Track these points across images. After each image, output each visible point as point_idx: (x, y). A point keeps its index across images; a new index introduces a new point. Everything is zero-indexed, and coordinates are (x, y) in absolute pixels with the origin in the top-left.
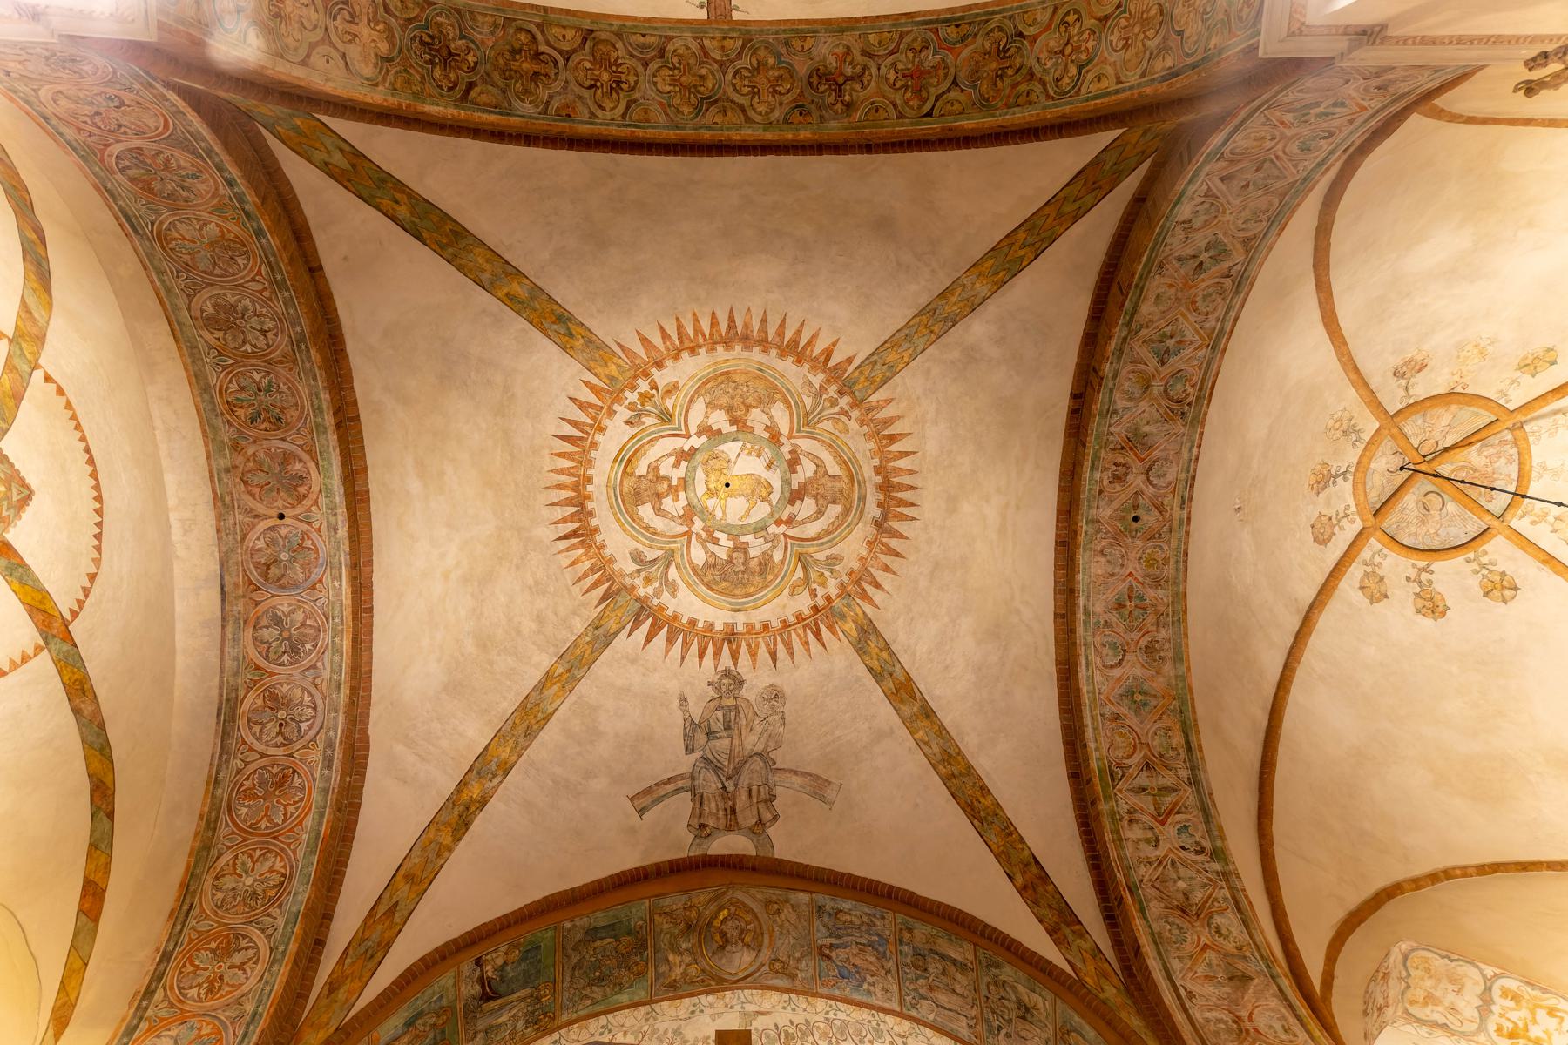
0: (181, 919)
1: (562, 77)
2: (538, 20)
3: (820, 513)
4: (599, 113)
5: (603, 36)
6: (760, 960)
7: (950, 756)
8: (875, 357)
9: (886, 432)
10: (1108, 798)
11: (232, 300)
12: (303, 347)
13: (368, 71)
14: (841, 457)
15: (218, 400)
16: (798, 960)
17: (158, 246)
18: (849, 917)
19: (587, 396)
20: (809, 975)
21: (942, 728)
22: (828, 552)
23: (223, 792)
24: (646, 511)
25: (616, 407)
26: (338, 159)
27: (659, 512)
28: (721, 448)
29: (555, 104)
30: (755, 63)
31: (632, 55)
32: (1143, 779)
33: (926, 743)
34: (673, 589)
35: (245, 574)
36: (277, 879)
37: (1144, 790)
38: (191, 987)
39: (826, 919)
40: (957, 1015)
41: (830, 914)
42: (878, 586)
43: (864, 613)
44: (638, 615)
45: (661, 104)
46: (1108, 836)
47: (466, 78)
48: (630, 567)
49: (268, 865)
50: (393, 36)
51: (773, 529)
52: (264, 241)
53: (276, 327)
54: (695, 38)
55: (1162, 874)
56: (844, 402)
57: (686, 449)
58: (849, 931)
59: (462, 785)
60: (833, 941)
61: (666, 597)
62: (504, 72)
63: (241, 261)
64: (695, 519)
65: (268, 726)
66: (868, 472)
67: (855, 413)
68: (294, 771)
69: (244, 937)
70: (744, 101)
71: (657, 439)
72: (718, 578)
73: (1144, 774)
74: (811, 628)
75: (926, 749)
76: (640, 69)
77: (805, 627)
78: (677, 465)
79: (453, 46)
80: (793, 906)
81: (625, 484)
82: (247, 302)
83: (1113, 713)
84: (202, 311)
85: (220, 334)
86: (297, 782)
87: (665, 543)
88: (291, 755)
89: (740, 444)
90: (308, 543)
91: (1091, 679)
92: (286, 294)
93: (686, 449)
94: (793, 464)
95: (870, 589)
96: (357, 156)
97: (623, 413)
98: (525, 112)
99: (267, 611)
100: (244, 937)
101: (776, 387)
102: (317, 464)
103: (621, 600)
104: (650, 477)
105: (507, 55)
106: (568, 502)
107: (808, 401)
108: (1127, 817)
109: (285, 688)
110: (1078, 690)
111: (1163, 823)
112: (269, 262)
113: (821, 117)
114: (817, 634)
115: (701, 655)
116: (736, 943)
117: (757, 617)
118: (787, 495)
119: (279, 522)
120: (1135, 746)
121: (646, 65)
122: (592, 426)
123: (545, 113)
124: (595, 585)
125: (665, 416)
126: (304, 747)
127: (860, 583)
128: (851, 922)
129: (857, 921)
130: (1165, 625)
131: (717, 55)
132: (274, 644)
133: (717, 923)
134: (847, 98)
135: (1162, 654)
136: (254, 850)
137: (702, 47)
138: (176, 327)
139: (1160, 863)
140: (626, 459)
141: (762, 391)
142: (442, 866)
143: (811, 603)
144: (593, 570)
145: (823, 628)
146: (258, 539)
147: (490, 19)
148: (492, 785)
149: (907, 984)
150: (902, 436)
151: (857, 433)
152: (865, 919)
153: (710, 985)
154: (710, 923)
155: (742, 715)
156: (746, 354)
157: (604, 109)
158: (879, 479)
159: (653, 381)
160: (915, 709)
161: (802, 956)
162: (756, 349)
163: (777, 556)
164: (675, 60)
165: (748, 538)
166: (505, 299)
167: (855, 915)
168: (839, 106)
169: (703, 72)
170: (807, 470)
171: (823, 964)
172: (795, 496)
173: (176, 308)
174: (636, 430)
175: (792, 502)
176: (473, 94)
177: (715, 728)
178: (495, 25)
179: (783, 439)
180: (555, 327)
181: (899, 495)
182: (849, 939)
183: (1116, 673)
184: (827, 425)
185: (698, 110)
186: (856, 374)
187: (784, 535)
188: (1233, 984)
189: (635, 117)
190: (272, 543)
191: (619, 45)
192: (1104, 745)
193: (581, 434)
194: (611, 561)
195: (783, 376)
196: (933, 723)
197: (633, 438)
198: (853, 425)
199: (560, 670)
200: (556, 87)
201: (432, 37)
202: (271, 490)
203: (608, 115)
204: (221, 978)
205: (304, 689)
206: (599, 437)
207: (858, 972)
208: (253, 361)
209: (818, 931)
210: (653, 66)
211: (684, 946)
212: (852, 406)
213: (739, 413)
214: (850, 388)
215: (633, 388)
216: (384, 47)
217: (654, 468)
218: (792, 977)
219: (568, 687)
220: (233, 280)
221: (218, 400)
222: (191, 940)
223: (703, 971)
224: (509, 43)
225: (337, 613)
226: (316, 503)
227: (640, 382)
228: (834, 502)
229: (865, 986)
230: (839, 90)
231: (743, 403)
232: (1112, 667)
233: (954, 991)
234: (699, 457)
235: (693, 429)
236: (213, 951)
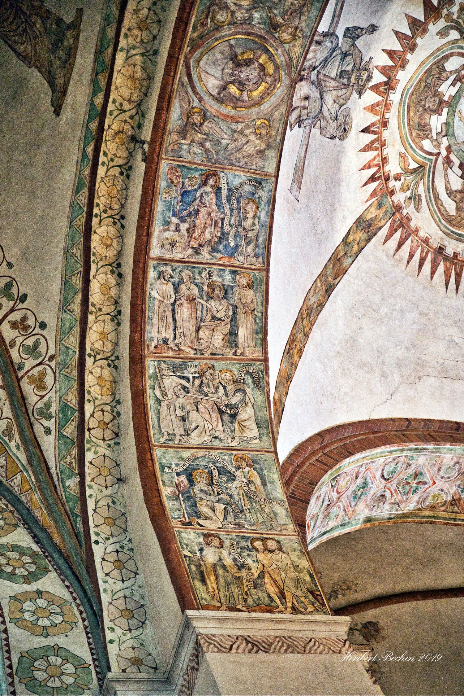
3: (450, 193)
6: (206, 98)
16: (202, 144)
18: (250, 215)
20: (184, 154)
22: (423, 198)
34: (442, 33)
39: (248, 188)
40: (172, 326)
41: (253, 194)
43: (381, 228)
51: (445, 142)
58: (236, 213)
60: (224, 192)
80: (262, 152)
95: (397, 235)
116: (232, 74)
128: (246, 217)
129: (248, 224)
130: (392, 508)
133: (263, 59)
135: (376, 507)
143: (392, 174)
149: (187, 272)
152: (251, 234)
153: (194, 30)
154: (266, 51)
161: (207, 151)
163: (427, 144)
167: (254, 223)
171: (197, 174)
182: (227, 211)
207: (190, 213)
209: (235, 176)
211: (256, 15)
218: (183, 133)
223: (218, 28)
228: (457, 209)
229: (175, 220)
233: (198, 328)
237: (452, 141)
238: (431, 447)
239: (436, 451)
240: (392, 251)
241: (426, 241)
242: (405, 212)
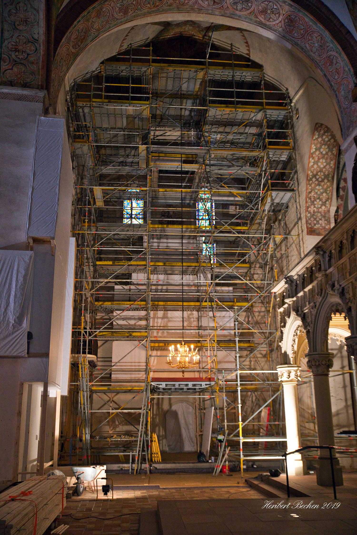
11: (117, 9)
35: (217, 9)
36: (319, 38)
49: (314, 37)
65: (272, 17)
68: (289, 16)
82: (118, 5)
85: (130, 10)
132: (244, 6)
136: (308, 38)
146: (204, 3)
204: (337, 69)
220: (111, 10)
221: (153, 9)
236: (330, 65)
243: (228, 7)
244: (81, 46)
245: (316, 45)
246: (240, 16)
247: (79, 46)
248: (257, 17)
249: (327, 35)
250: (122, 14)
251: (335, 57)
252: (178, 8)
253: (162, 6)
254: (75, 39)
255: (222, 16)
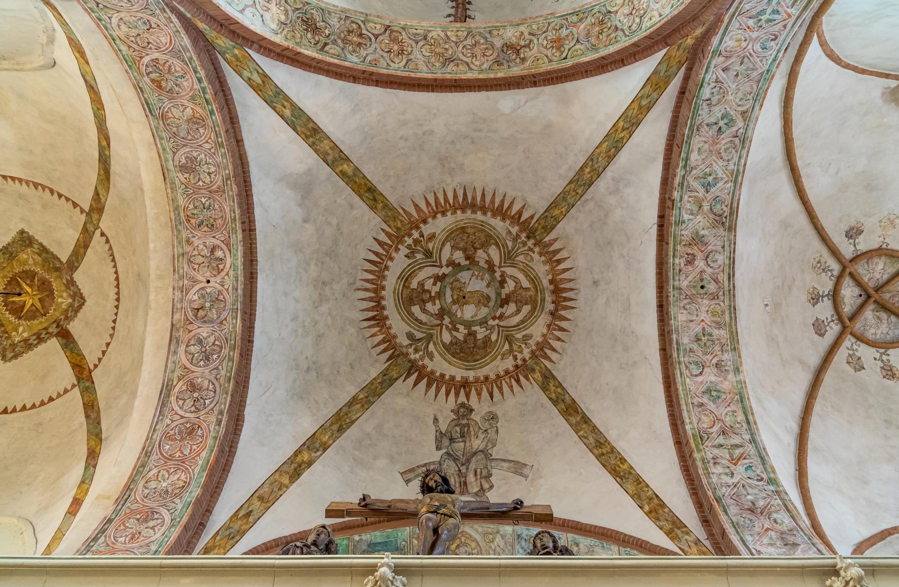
0: (122, 502)
1: (374, 46)
2: (362, 19)
3: (518, 311)
4: (392, 64)
5: (395, 29)
7: (601, 443)
8: (547, 214)
9: (555, 258)
10: (699, 450)
11: (195, 154)
12: (229, 182)
13: (274, 26)
14: (530, 276)
15: (182, 214)
17: (161, 122)
19: (383, 238)
21: (595, 427)
22: (524, 333)
23: (157, 437)
24: (416, 309)
25: (400, 246)
26: (257, 79)
27: (424, 311)
28: (460, 274)
29: (369, 58)
30: (474, 42)
31: (410, 38)
32: (721, 440)
33: (585, 437)
34: (431, 357)
35: (185, 315)
36: (181, 484)
37: (722, 446)
38: (121, 537)
42: (554, 350)
43: (546, 367)
44: (409, 370)
45: (424, 62)
46: (701, 472)
47: (323, 40)
48: (406, 342)
49: (177, 476)
50: (288, 14)
51: (491, 322)
52: (214, 118)
53: (216, 171)
54: (443, 31)
55: (737, 492)
56: (530, 243)
57: (440, 274)
59: (297, 453)
61: (427, 361)
62: (343, 40)
63: (201, 130)
64: (445, 317)
65: (187, 401)
66: (545, 282)
67: (537, 249)
68: (199, 427)
69: (157, 513)
70: (468, 60)
71: (423, 267)
72: (458, 351)
73: (721, 437)
74: (514, 378)
75: (585, 441)
76: (414, 45)
77: (510, 377)
78: (435, 284)
79: (318, 25)
81: (404, 292)
82: (202, 156)
83: (699, 402)
84: (180, 162)
85: (187, 175)
86: (200, 432)
87: (427, 329)
88: (197, 418)
89: (471, 272)
90: (221, 297)
91: (684, 384)
92: (223, 150)
93: (440, 274)
94: (502, 283)
95: (548, 352)
96: (265, 76)
97: (404, 250)
98: (353, 61)
99: (195, 336)
100: (157, 513)
101: (491, 236)
102: (230, 251)
103: (399, 360)
104: (419, 290)
105: (346, 33)
106: (370, 299)
107: (510, 244)
108: (712, 461)
109: (199, 380)
110: (677, 390)
111: (735, 464)
112: (216, 131)
113: (509, 66)
114: (518, 381)
115: (447, 394)
117: (481, 373)
118: (499, 302)
119: (206, 285)
120: (714, 422)
121: (417, 43)
122: (386, 256)
123: (364, 62)
124: (384, 351)
125: (428, 254)
126: (206, 413)
127: (542, 349)
131: (454, 39)
132: (196, 355)
134: (522, 56)
136: (170, 468)
137: (447, 35)
138: (166, 171)
139: (735, 486)
140: (406, 278)
141: (483, 238)
142: (281, 495)
143: (514, 363)
144: (383, 341)
145: (521, 378)
146: (194, 294)
147: (338, 15)
148: (316, 455)
150: (565, 259)
151: (539, 261)
155: (471, 429)
156: (473, 216)
157: (394, 63)
158: (552, 287)
159: (421, 231)
160: (578, 419)
162: (479, 213)
163: (494, 337)
164: (432, 41)
165: (476, 328)
166: (339, 174)
168: (518, 60)
169: (447, 46)
170: (510, 285)
172: (504, 302)
173: (167, 160)
174: (411, 261)
175: (502, 306)
176: (327, 48)
177: (454, 435)
178: (341, 19)
179: (496, 269)
180: (367, 194)
181: (564, 295)
183: (699, 379)
184: (521, 258)
185: (444, 64)
186: (536, 225)
187: (498, 325)
188: (787, 547)
189: (410, 67)
190: (203, 296)
191: (404, 33)
192: (695, 421)
193: (379, 260)
194: (395, 337)
195: (494, 229)
196: (589, 425)
197: (409, 265)
198: (536, 256)
199: (361, 396)
200: (371, 50)
201: (308, 19)
202: (205, 266)
203: (397, 66)
204: (140, 533)
205: (210, 381)
206: (389, 263)
208: (203, 191)
210: (421, 44)
212: (535, 245)
213: (470, 253)
214: (533, 234)
215: (410, 235)
216: (283, 18)
217: (421, 284)
219: (366, 406)
220: (197, 143)
221: (182, 214)
222: (126, 514)
224: (347, 27)
225: (233, 338)
226: (227, 274)
227: (414, 232)
228: (527, 304)
230: (518, 52)
231: (473, 246)
232: (696, 376)
234: (447, 280)
235: (444, 263)
236: (138, 520)
237: (489, 317)
238: (674, 337)
239: (677, 331)
240: (558, 356)
241: (549, 326)
242: (534, 348)
243: (190, 331)
244: (146, 79)
245: (165, 484)
246: (175, 353)
247: (148, 74)
248: (179, 380)
249: (195, 492)
250: (184, 161)
251: (159, 521)
252: (183, 255)
253: (187, 229)
254: (170, 66)
255: (173, 325)
